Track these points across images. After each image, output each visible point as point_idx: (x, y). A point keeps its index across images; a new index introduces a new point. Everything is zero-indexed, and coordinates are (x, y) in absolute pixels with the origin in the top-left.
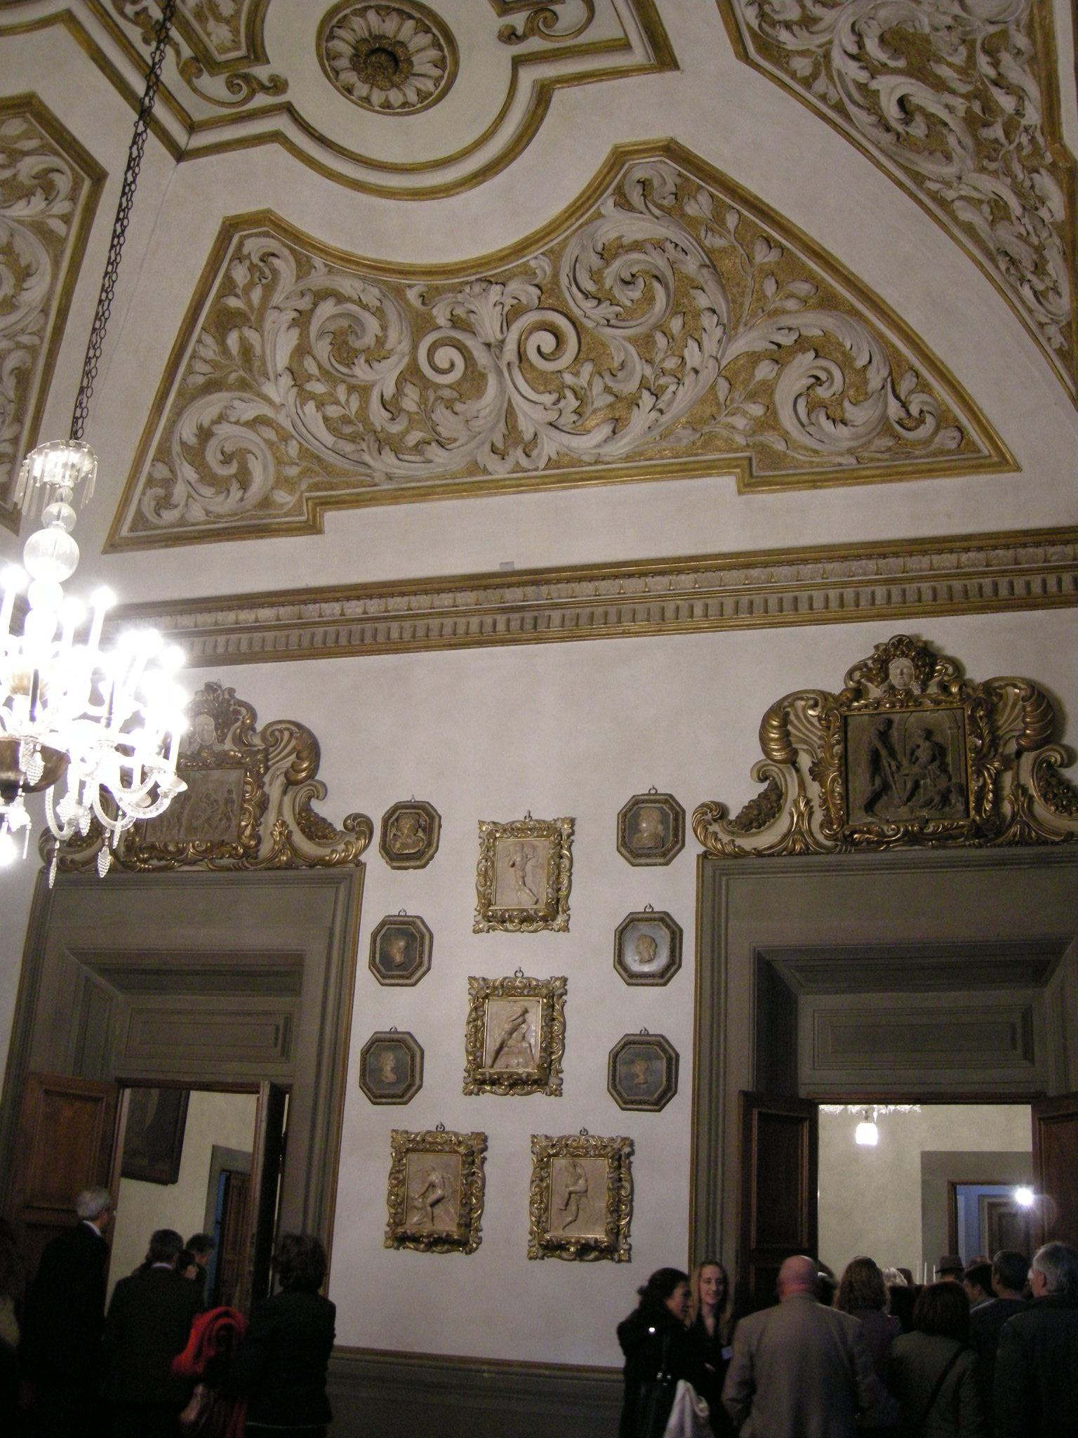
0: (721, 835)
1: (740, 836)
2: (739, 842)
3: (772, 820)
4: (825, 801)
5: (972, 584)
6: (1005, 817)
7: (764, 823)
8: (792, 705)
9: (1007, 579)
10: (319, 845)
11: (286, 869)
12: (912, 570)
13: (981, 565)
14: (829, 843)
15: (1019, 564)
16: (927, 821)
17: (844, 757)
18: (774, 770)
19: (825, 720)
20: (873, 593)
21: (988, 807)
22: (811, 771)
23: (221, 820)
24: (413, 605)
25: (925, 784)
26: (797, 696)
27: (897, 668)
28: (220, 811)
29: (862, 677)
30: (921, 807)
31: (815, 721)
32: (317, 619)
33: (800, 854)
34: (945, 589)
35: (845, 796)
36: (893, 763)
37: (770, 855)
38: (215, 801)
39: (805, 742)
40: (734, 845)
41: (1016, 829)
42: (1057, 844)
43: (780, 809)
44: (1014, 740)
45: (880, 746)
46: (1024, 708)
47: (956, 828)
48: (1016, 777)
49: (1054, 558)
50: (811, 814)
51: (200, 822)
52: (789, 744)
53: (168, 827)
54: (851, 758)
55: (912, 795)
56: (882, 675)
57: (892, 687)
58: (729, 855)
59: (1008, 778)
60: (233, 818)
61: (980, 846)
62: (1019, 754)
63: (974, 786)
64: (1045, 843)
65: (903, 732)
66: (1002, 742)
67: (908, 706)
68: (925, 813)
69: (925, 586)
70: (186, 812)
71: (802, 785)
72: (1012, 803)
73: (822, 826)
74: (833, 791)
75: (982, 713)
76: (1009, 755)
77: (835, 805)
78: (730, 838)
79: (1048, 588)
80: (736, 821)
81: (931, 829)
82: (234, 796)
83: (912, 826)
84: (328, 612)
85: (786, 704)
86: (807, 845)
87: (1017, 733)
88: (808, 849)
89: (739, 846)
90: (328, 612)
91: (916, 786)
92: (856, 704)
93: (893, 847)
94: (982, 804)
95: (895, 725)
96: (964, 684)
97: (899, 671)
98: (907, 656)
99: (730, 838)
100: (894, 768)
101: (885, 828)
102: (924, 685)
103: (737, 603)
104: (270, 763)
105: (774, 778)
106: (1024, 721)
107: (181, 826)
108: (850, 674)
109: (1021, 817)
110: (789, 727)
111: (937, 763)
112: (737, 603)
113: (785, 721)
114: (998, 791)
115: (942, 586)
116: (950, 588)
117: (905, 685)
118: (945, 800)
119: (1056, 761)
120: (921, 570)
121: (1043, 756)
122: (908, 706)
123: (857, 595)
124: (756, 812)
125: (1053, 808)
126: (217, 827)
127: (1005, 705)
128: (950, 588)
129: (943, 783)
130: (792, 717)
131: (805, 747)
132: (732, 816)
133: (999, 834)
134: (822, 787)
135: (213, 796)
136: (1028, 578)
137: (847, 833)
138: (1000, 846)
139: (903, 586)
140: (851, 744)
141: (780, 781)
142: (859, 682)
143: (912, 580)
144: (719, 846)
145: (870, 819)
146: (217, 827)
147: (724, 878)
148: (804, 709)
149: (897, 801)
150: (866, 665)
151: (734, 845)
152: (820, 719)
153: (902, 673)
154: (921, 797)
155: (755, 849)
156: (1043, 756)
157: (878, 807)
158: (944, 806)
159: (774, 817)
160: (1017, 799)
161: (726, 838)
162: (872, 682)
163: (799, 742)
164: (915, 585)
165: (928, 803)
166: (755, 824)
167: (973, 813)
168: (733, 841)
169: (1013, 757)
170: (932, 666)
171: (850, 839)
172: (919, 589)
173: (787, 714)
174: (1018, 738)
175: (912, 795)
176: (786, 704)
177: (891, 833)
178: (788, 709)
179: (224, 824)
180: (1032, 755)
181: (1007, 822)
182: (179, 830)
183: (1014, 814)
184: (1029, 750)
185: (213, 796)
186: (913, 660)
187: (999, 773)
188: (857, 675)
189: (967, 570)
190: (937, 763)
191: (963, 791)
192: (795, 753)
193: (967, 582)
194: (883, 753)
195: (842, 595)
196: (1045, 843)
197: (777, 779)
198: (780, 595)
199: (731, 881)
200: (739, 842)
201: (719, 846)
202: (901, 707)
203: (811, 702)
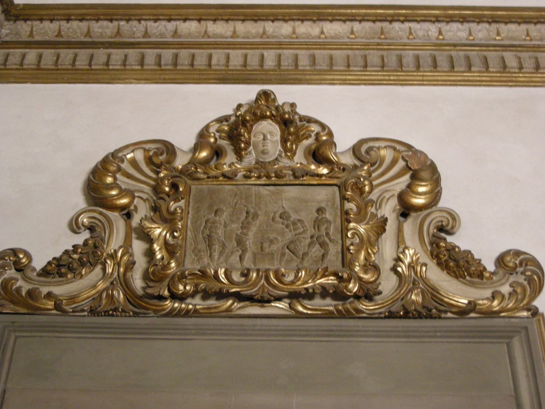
10: (472, 284)
11: (420, 316)
23: (310, 245)
24: (533, 34)
28: (309, 234)
32: (405, 41)
38: (300, 220)
51: (274, 247)
53: (221, 254)
60: (331, 245)
70: (251, 234)
82: (328, 216)
84: (421, 33)
90: (421, 33)
104: (374, 183)
107: (244, 251)
126: (305, 254)
135: (294, 216)
146: (305, 254)
179: (316, 250)
182: (241, 258)
185: (294, 216)
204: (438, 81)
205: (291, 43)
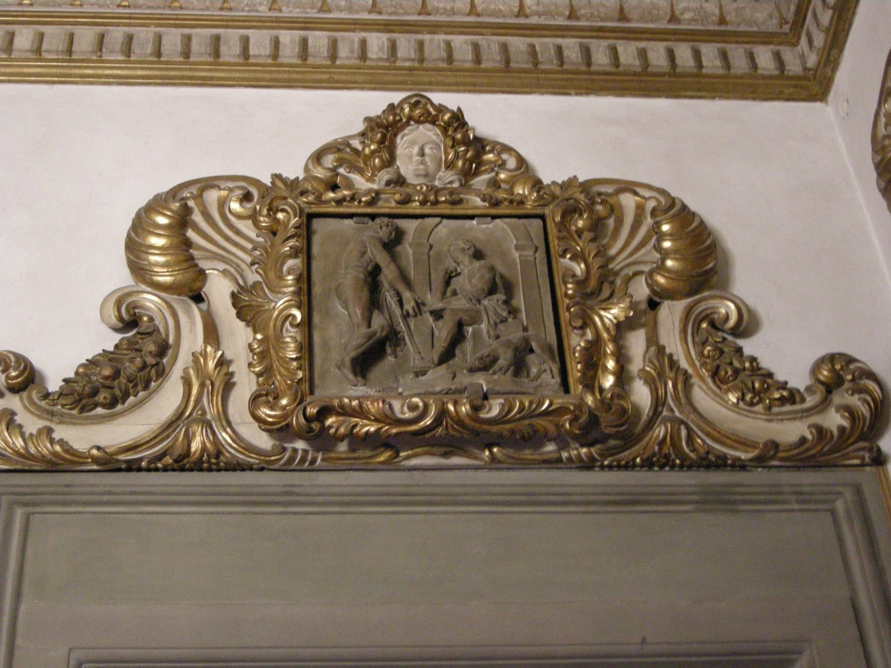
0: (22, 417)
1: (64, 420)
2: (61, 432)
3: (141, 394)
4: (263, 356)
5: (545, 44)
6: (637, 410)
7: (126, 395)
8: (199, 197)
9: (605, 43)
12: (437, 11)
13: (560, 14)
14: (263, 441)
15: (627, 20)
16: (485, 397)
17: (305, 281)
18: (151, 300)
19: (268, 215)
20: (363, 43)
21: (609, 381)
22: (234, 296)
25: (477, 335)
26: (209, 183)
27: (412, 143)
29: (341, 162)
30: (472, 370)
31: (246, 227)
33: (198, 466)
34: (495, 48)
35: (307, 348)
36: (407, 295)
37: (132, 467)
39: (223, 259)
40: (52, 441)
41: (660, 431)
42: (740, 466)
43: (162, 373)
44: (643, 279)
45: (382, 258)
46: (656, 229)
47: (546, 413)
48: (652, 340)
49: (687, 16)
50: (229, 385)
52: (191, 258)
54: (317, 289)
55: (447, 355)
56: (386, 156)
57: (400, 181)
58: (42, 459)
59: (637, 342)
61: (588, 465)
62: (653, 305)
63: (577, 342)
64: (721, 463)
65: (426, 251)
66: (618, 282)
67: (436, 203)
68: (482, 381)
69: (458, 40)
71: (212, 333)
72: (650, 382)
73: (255, 400)
74: (279, 337)
75: (580, 223)
76: (639, 302)
77: (286, 361)
78: (42, 423)
79: (679, 61)
80: (61, 394)
81: (495, 412)
83: (455, 403)
85: (186, 194)
86: (216, 442)
87: (646, 268)
88: (218, 454)
89: (61, 442)
91: (458, 337)
92: (331, 195)
93: (407, 458)
94: (595, 377)
95: (409, 238)
96: (537, 184)
97: (416, 150)
98: (433, 123)
99: (42, 423)
100: (409, 306)
101: (397, 405)
102: (468, 174)
103: (102, 37)
105: (151, 319)
106: (658, 248)
108: (318, 157)
109: (672, 411)
110: (191, 234)
111: (500, 296)
112: (102, 37)
113: (183, 221)
114: (622, 358)
115: (491, 44)
116: (504, 47)
117: (426, 175)
118: (519, 367)
119: (727, 318)
120: (453, 12)
121: (702, 306)
122: (436, 203)
123: (334, 44)
124: (107, 372)
125: (733, 398)
127: (620, 222)
128: (504, 47)
129: (514, 334)
130: (197, 217)
131: (222, 266)
132: (54, 385)
133: (629, 439)
134: (255, 332)
136: (642, 44)
137: (312, 411)
138: (629, 466)
139: (419, 37)
140: (317, 266)
141: (164, 322)
142: (334, 170)
143: (434, 28)
144: (19, 443)
145: (361, 390)
147: (19, 513)
148: (222, 204)
149: (415, 361)
150: (349, 145)
151: (52, 441)
152: (253, 217)
153: (422, 154)
154: (468, 352)
155: (99, 448)
156: (702, 306)
157: (379, 371)
158: (516, 374)
159: (146, 387)
160: (661, 374)
161: (32, 424)
162: (361, 172)
163: (206, 258)
164: (441, 37)
165: (487, 365)
166: (101, 397)
167: (577, 388)
168: (50, 431)
169: (644, 306)
170: (478, 158)
171: (316, 426)
172: (448, 44)
173: (186, 211)
174: (651, 274)
175: (447, 355)
176: (186, 194)
177: (408, 415)
178: (191, 203)
180: (680, 305)
181: (644, 418)
183: (658, 403)
184: (670, 295)
186: (445, 130)
187: (622, 328)
188: (329, 160)
189: (534, 20)
190: (500, 296)
191: (560, 353)
192: (202, 275)
193: (536, 41)
194: (389, 273)
195: (304, 42)
196: (721, 463)
197: (158, 321)
198: (186, 31)
199: (36, 520)
200: (61, 432)
201: (19, 443)
202: (423, 203)
203: (239, 192)
204: (70, 76)
205: (25, 14)
